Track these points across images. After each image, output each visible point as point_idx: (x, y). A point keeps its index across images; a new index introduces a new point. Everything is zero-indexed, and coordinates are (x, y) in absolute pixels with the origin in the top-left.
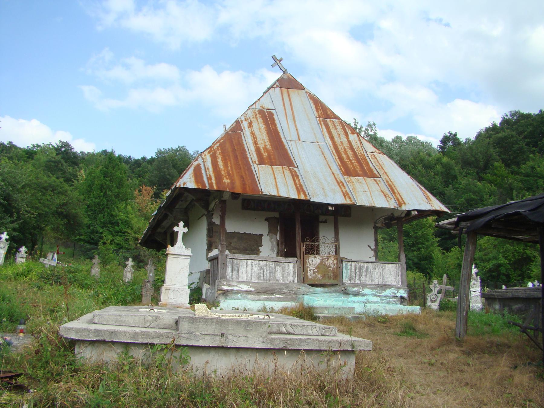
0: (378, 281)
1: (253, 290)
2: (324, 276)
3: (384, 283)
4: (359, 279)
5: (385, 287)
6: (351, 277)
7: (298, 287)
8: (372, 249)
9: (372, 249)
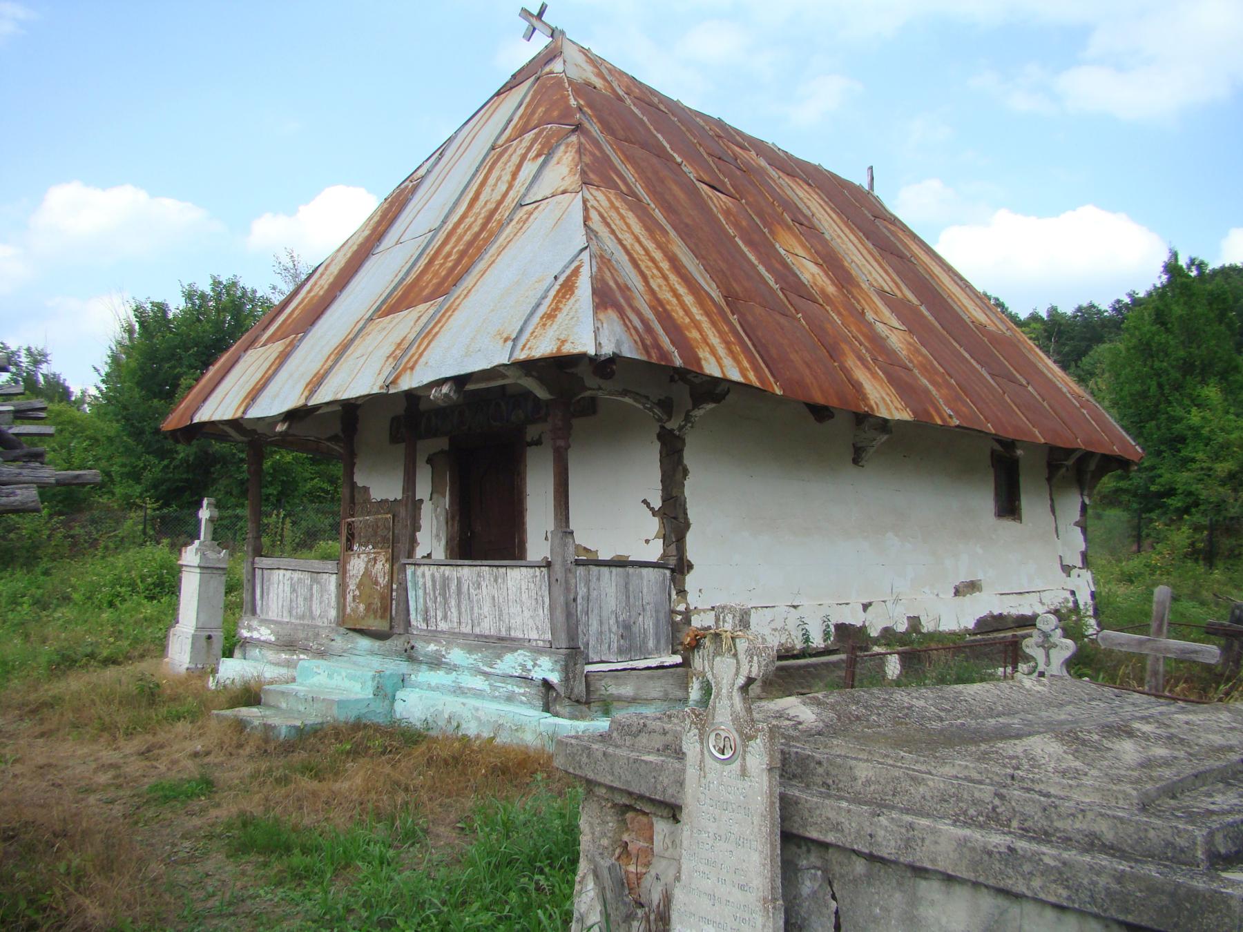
0: (487, 627)
1: (273, 639)
3: (504, 633)
4: (445, 618)
5: (503, 643)
6: (426, 611)
8: (652, 509)
9: (652, 509)
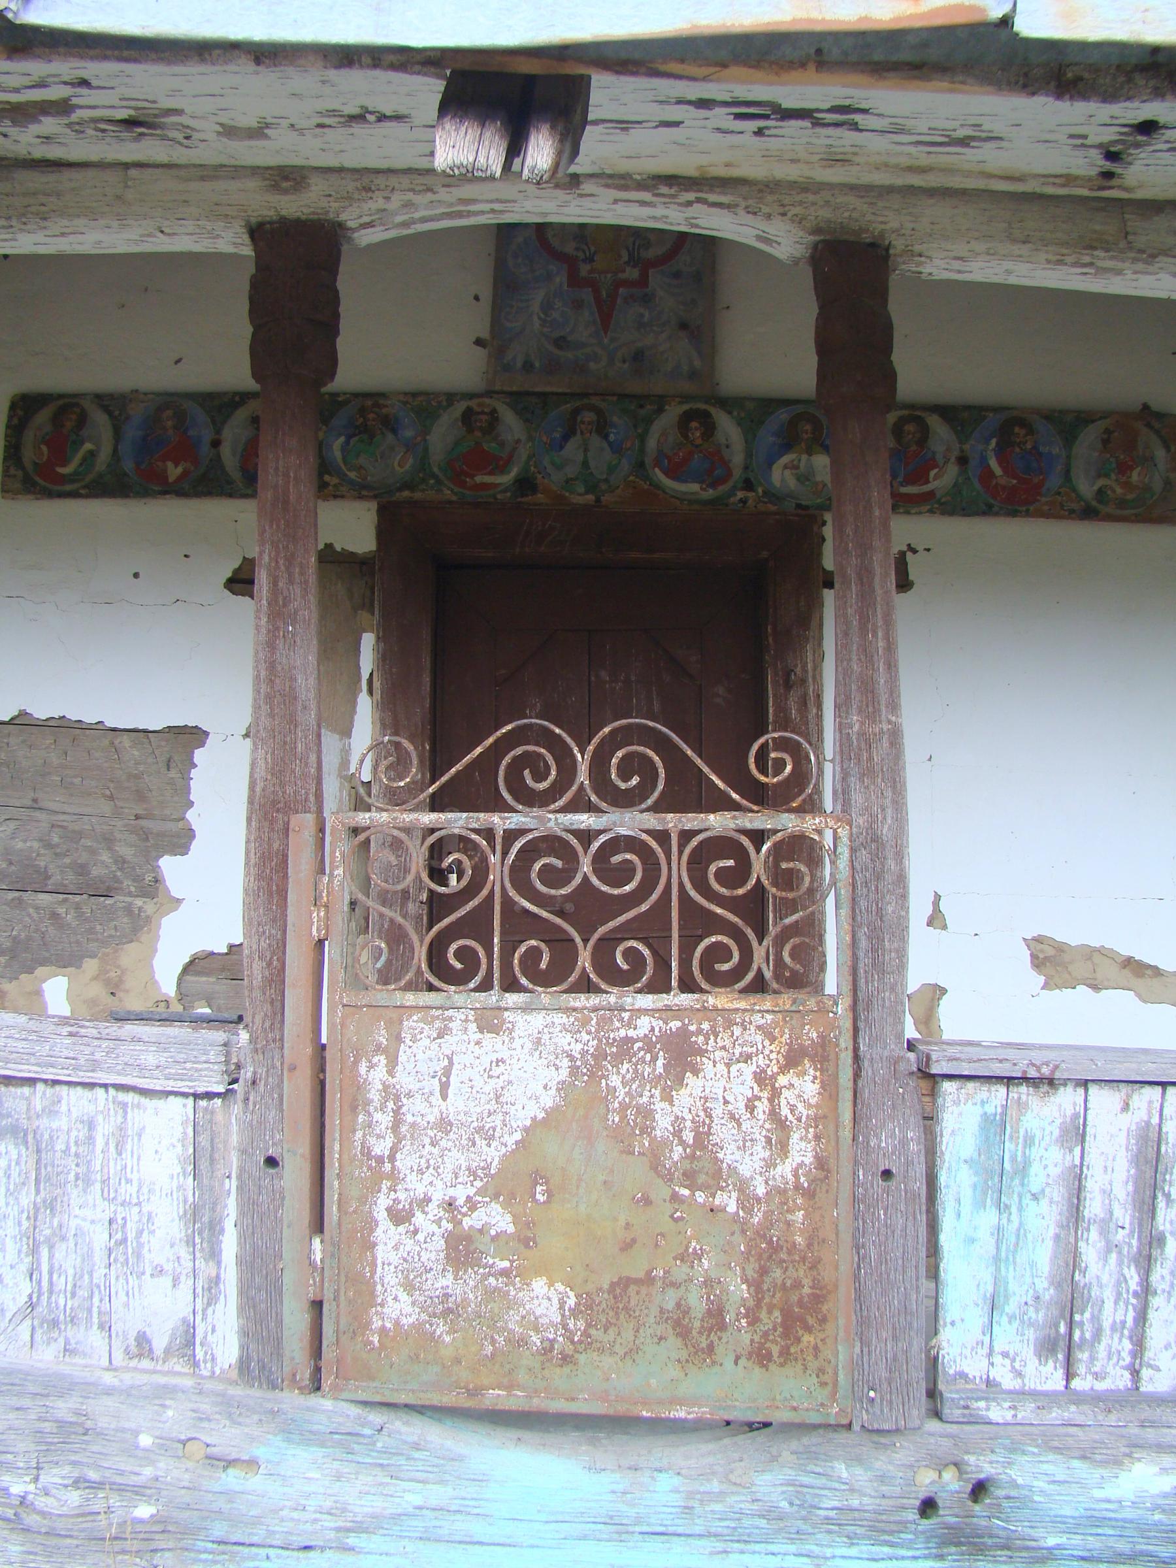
2: (611, 1304)
6: (1071, 1298)
7: (225, 1437)
